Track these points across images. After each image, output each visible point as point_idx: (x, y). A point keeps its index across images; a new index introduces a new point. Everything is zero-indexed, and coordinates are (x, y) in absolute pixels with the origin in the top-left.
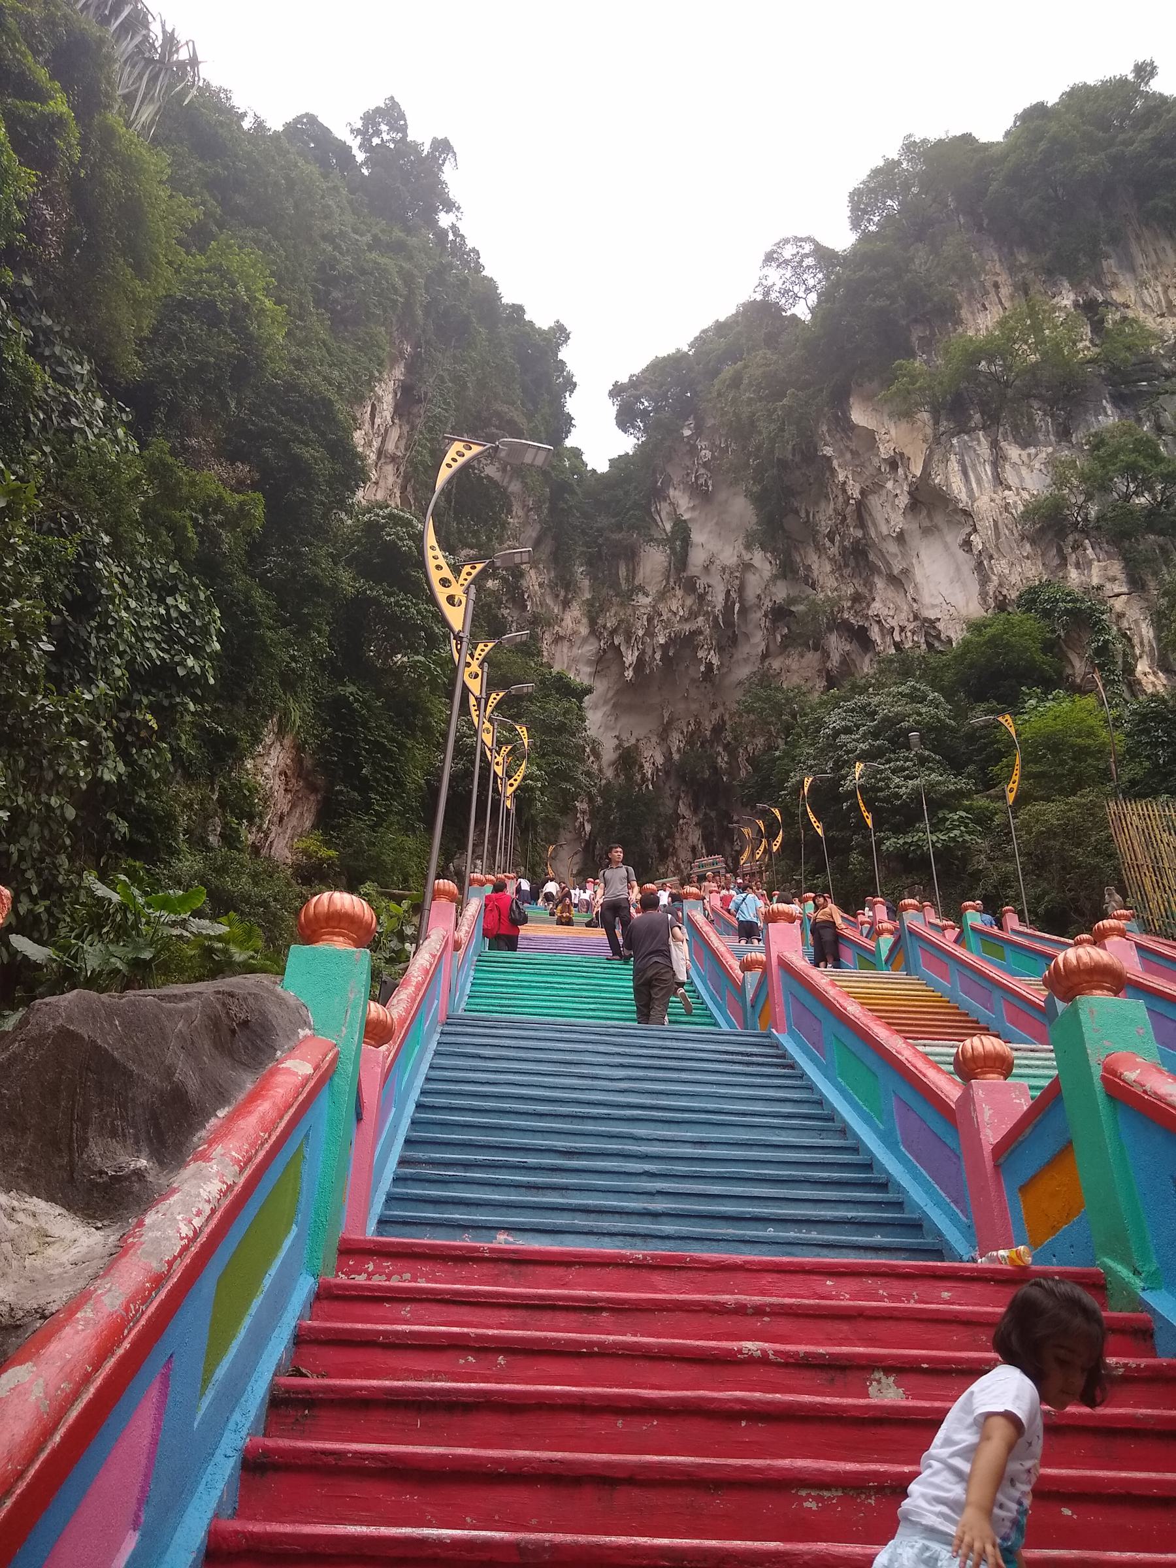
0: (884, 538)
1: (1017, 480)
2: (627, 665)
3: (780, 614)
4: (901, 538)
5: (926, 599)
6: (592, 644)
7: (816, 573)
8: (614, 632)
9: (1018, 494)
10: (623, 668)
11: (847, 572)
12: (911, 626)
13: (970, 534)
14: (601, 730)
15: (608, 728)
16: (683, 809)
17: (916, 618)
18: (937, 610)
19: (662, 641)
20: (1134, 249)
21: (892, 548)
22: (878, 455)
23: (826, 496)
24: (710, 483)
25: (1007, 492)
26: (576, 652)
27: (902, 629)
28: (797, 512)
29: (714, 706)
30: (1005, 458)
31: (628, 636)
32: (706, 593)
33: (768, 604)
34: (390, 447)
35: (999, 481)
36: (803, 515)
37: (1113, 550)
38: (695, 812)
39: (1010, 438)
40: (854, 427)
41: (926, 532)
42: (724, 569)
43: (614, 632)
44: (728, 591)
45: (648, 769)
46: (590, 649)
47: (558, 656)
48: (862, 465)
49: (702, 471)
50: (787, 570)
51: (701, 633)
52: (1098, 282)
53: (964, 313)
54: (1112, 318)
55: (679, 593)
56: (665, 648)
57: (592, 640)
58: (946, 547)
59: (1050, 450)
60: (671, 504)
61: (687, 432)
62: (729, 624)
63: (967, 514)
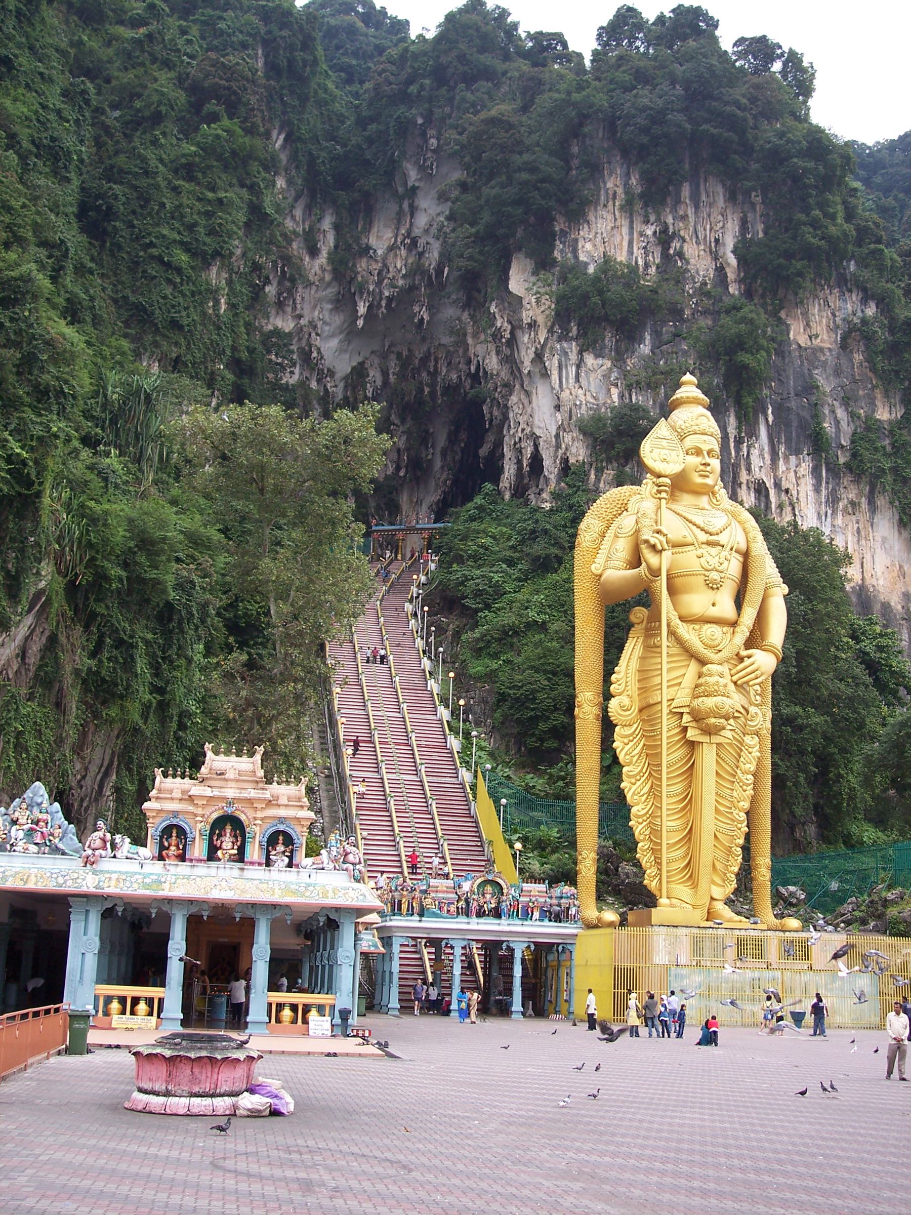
5: (536, 422)
10: (357, 318)
19: (387, 294)
20: (702, 188)
25: (580, 391)
29: (424, 339)
31: (362, 289)
38: (403, 421)
40: (510, 293)
46: (332, 291)
48: (514, 312)
49: (429, 155)
52: (674, 210)
53: (591, 217)
54: (675, 245)
55: (403, 252)
56: (390, 300)
57: (335, 284)
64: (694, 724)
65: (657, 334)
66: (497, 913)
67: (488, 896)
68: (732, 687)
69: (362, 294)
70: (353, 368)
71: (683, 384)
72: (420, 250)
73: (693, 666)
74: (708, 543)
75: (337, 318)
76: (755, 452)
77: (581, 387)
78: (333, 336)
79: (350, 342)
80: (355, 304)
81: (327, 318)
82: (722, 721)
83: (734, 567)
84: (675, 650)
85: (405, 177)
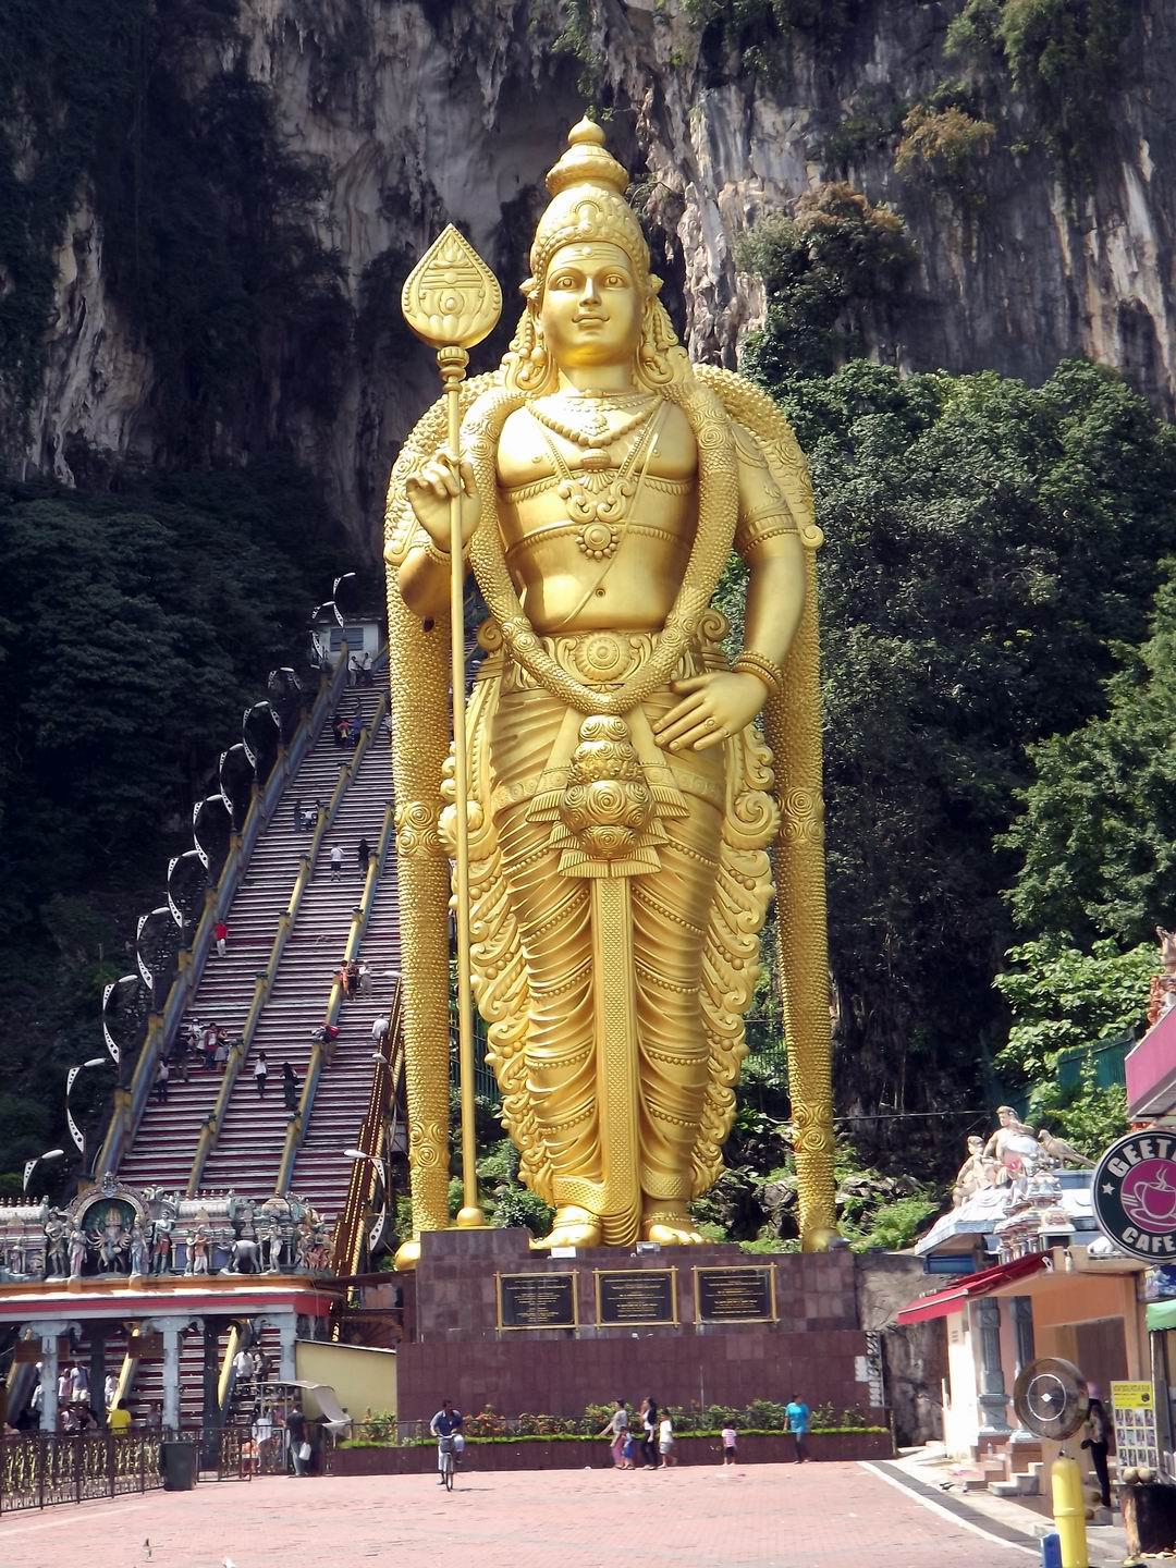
1: (764, 168)
2: (486, 102)
6: (436, 59)
14: (469, 187)
15: (478, 181)
25: (754, 184)
26: (415, 74)
31: (484, 48)
39: (768, 94)
47: (387, 85)
57: (439, 50)
64: (573, 843)
65: (899, 34)
66: (123, 1263)
67: (112, 1232)
68: (651, 756)
69: (487, 59)
70: (506, 208)
71: (576, 141)
73: (570, 718)
74: (585, 466)
75: (456, 117)
76: (1117, 246)
77: (754, 175)
78: (455, 153)
79: (492, 161)
81: (436, 122)
82: (618, 830)
83: (657, 505)
84: (537, 696)
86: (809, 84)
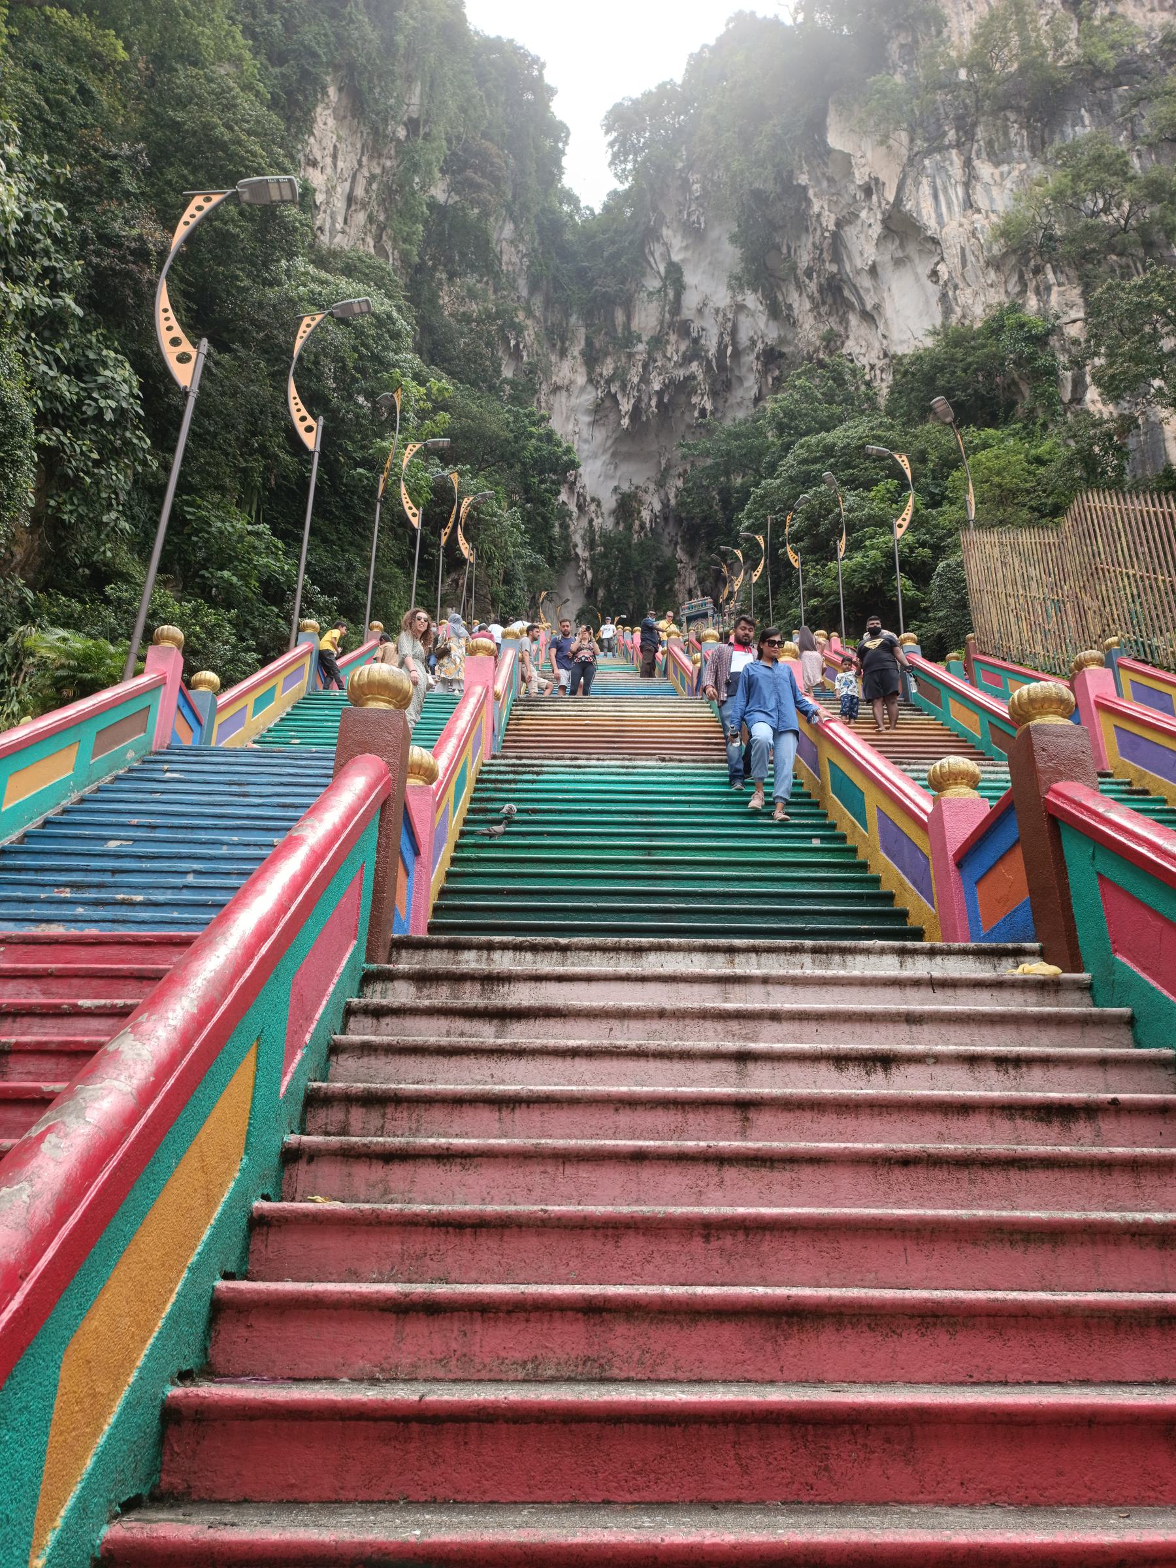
0: (858, 272)
1: (987, 202)
3: (771, 357)
4: (873, 271)
5: (895, 335)
7: (796, 312)
8: (609, 382)
9: (987, 217)
11: (824, 310)
12: (880, 364)
13: (937, 264)
15: (608, 477)
16: (680, 554)
17: (886, 355)
18: (905, 346)
19: (657, 387)
21: (865, 282)
22: (853, 182)
23: (807, 231)
24: (702, 219)
25: (976, 216)
26: (574, 401)
27: (872, 367)
28: (779, 249)
30: (976, 178)
32: (700, 337)
33: (760, 346)
34: (359, 192)
35: (969, 204)
36: (784, 250)
37: (1072, 273)
38: (692, 555)
39: (984, 155)
40: (830, 151)
41: (898, 262)
42: (717, 311)
43: (609, 382)
44: (722, 334)
45: (646, 515)
46: (589, 397)
47: (556, 406)
48: (838, 194)
50: (777, 311)
51: (695, 378)
55: (673, 338)
56: (660, 394)
57: (590, 388)
58: (917, 279)
59: (1023, 166)
60: (665, 244)
61: (680, 165)
62: (722, 367)
63: (935, 242)
72: (695, 335)
77: (979, 211)
78: (595, 456)
80: (617, 403)
85: (668, 247)
86: (1023, 147)
